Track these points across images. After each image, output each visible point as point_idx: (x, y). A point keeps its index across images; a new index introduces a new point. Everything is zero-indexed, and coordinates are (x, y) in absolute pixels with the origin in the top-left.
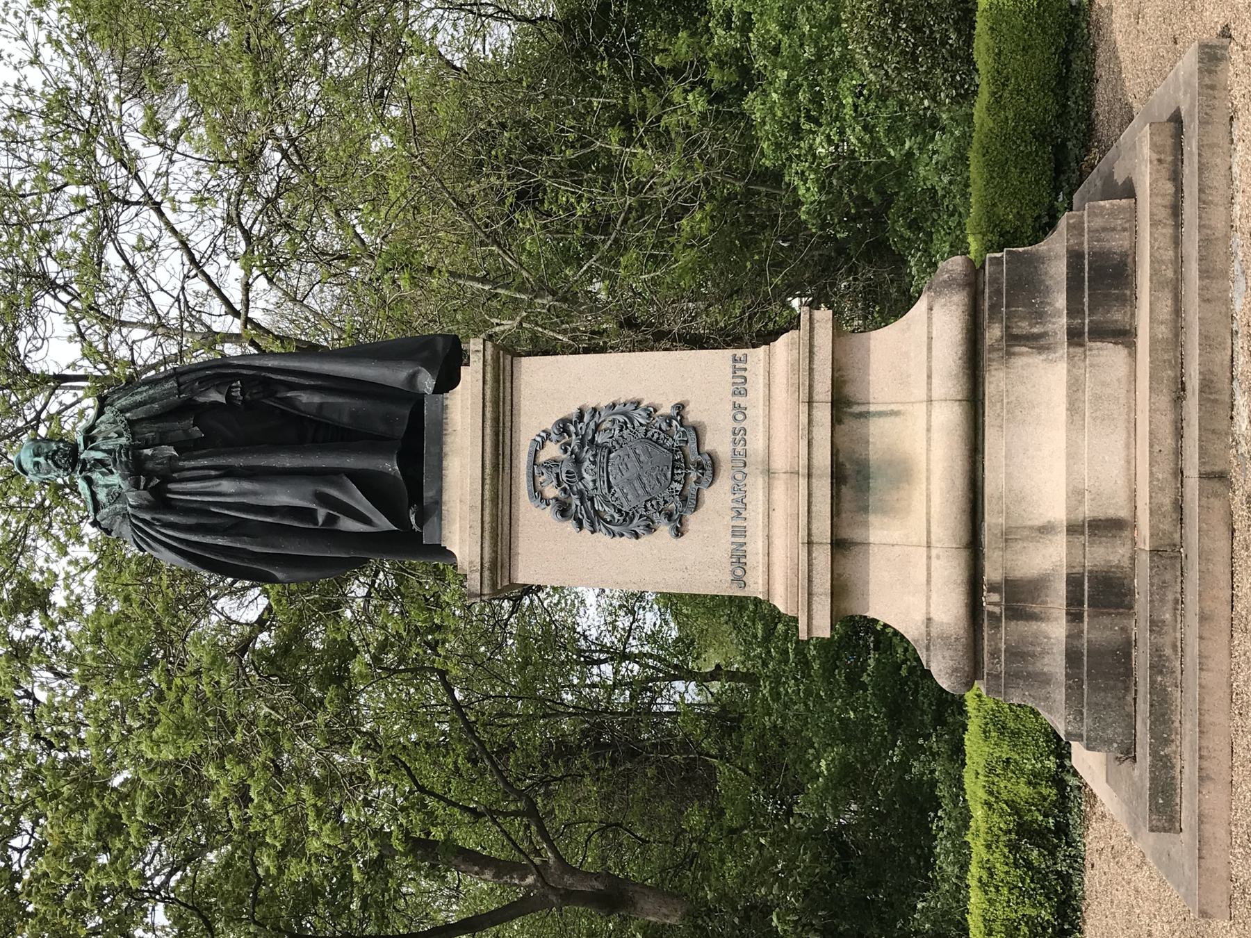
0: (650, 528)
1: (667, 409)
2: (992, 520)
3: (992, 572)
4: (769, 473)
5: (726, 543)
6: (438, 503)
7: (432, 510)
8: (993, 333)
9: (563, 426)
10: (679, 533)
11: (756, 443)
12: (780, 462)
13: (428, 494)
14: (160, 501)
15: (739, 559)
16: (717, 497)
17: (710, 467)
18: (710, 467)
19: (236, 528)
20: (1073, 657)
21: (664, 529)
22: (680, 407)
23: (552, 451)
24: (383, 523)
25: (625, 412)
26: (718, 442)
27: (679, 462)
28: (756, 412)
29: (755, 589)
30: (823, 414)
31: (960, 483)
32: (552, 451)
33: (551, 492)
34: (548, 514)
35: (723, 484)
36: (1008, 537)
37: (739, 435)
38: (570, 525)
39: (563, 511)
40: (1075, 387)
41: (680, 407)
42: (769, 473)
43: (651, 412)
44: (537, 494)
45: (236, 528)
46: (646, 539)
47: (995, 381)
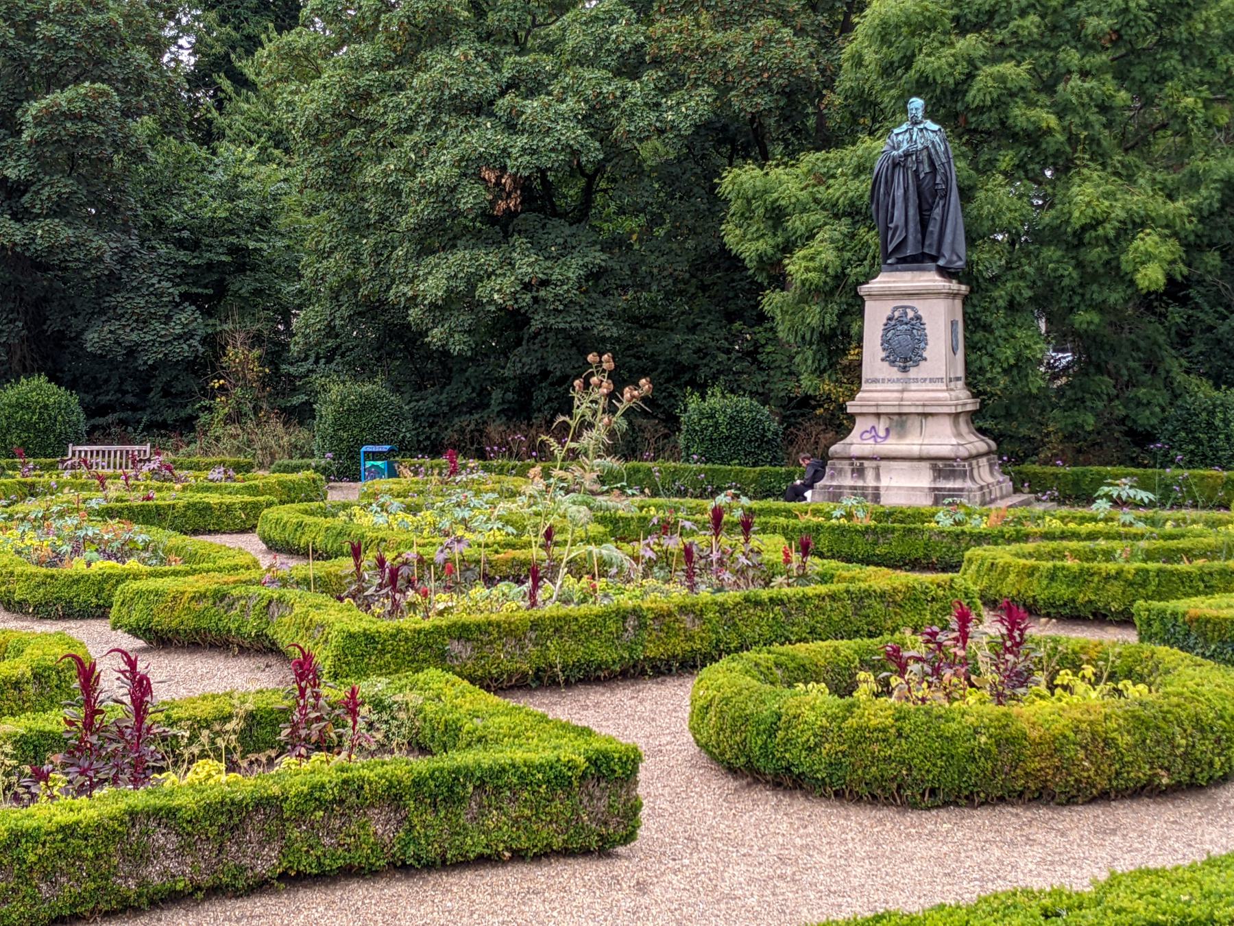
0: (884, 350)
1: (925, 355)
2: (883, 463)
3: (866, 463)
4: (903, 391)
5: (880, 376)
6: (897, 270)
7: (892, 268)
8: (940, 464)
9: (919, 318)
10: (883, 360)
11: (913, 386)
12: (906, 395)
13: (899, 266)
14: (896, 165)
15: (875, 381)
16: (894, 373)
17: (905, 369)
18: (905, 369)
19: (887, 193)
20: (840, 487)
21: (883, 355)
22: (925, 359)
23: (911, 314)
24: (890, 249)
25: (923, 339)
26: (913, 373)
27: (906, 360)
28: (924, 386)
29: (864, 386)
30: (920, 410)
31: (894, 454)
32: (911, 314)
33: (897, 314)
34: (889, 313)
35: (899, 375)
36: (877, 468)
37: (916, 380)
38: (885, 321)
39: (890, 319)
40: (921, 489)
41: (925, 359)
42: (903, 391)
43: (924, 349)
44: (896, 308)
45: (887, 193)
46: (880, 348)
47: (926, 464)
